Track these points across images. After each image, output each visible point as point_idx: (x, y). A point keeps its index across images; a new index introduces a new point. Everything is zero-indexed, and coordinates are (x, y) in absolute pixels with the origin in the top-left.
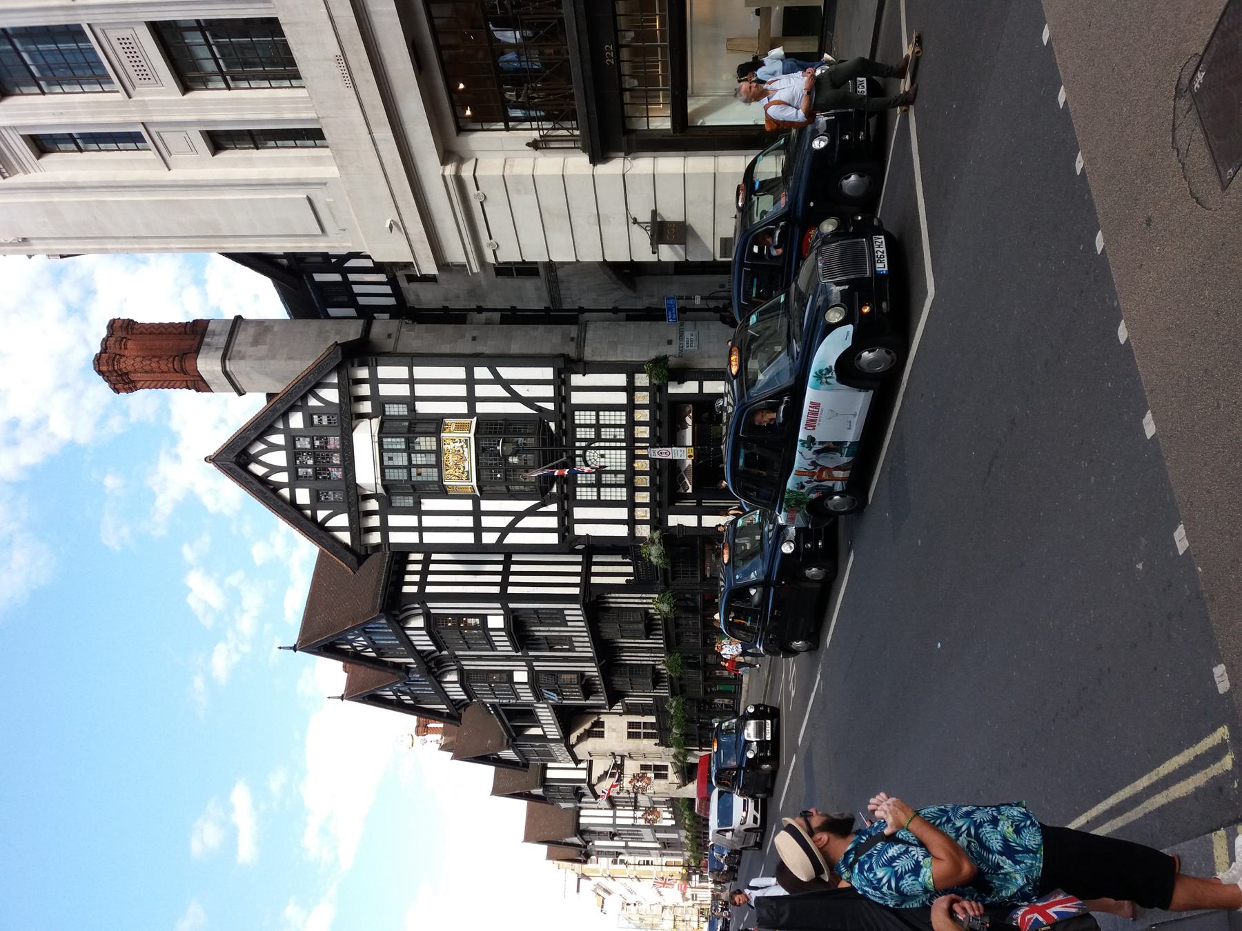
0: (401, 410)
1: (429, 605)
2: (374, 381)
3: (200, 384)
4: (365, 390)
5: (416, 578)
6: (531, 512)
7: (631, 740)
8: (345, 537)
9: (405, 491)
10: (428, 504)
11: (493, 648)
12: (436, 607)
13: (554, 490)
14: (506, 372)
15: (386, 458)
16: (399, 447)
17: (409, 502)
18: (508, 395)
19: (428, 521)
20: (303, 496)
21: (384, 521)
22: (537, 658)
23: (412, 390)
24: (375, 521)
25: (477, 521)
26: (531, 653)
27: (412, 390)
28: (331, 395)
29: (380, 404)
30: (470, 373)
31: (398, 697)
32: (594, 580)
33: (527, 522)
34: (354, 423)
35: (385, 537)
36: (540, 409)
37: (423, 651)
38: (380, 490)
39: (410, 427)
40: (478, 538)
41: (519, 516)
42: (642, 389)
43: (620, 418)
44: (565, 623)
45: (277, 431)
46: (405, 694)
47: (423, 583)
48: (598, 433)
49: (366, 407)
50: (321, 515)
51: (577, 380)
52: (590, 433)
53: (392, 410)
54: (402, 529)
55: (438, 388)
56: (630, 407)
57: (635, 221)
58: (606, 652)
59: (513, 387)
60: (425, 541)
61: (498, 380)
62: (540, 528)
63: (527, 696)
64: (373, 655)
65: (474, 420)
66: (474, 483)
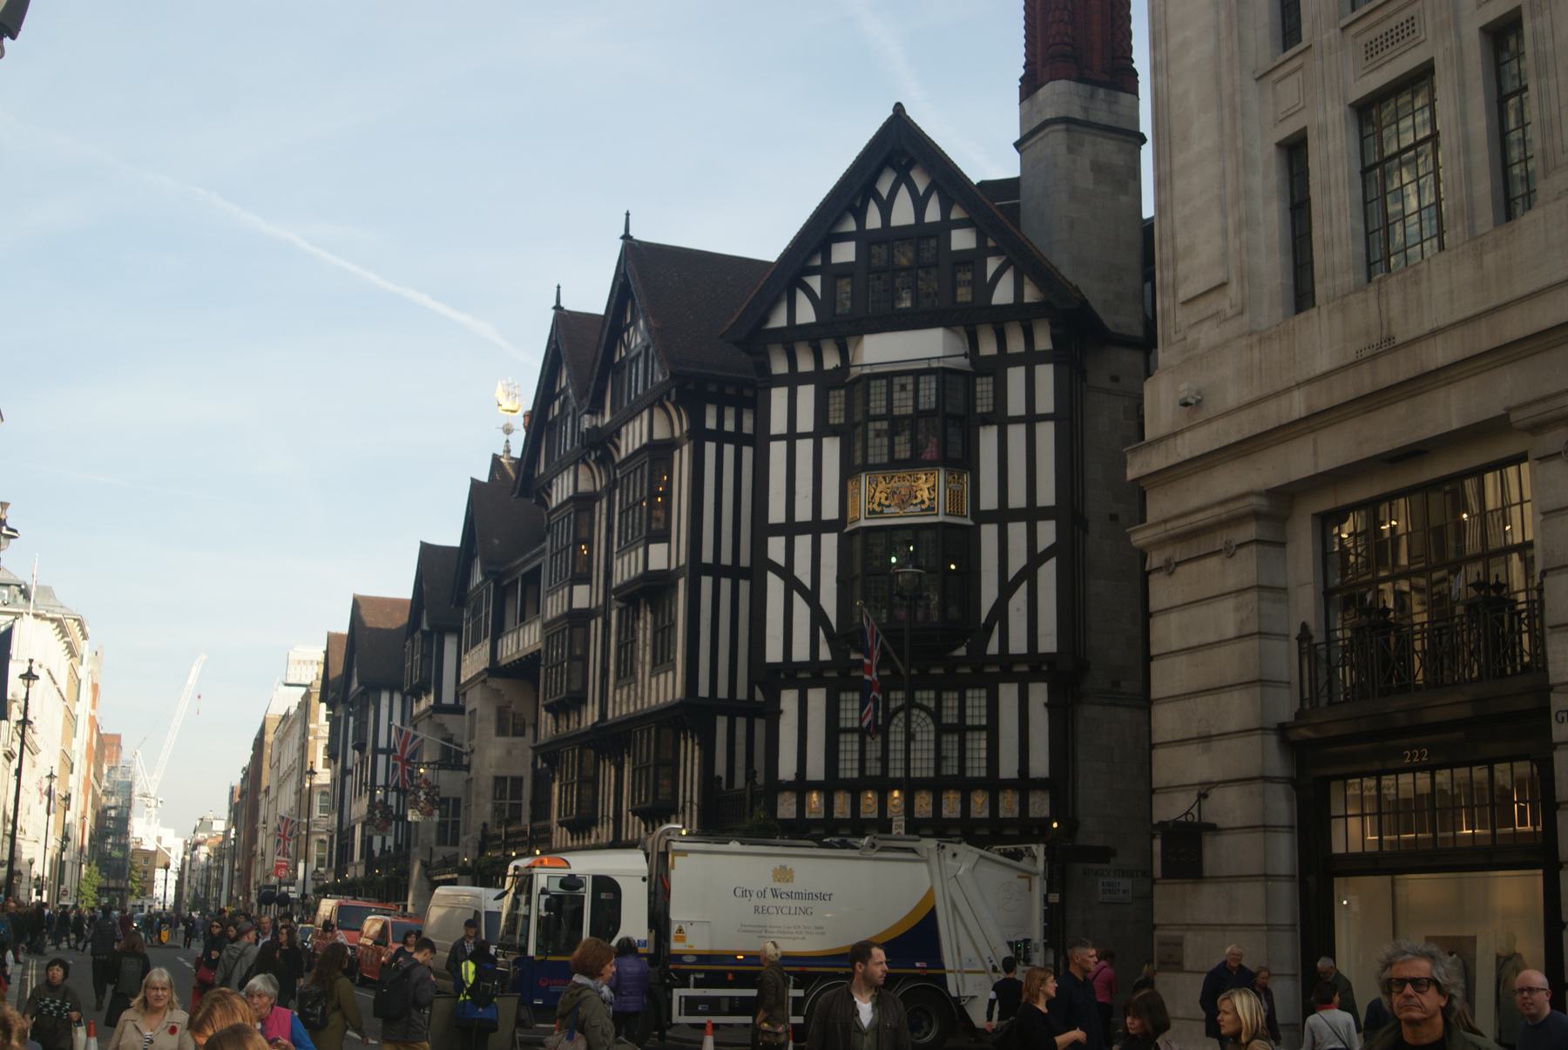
0: (984, 405)
1: (686, 448)
2: (1030, 359)
3: (1029, 86)
4: (1016, 345)
5: (729, 426)
6: (818, 617)
7: (491, 782)
8: (779, 320)
9: (853, 411)
10: (831, 447)
11: (621, 553)
12: (682, 460)
14: (1048, 574)
15: (903, 380)
16: (921, 400)
17: (836, 418)
18: (1012, 573)
19: (804, 448)
20: (844, 253)
21: (806, 379)
22: (607, 624)
23: (1017, 420)
24: (806, 364)
25: (803, 528)
26: (614, 614)
27: (1017, 420)
28: (1003, 294)
29: (995, 369)
30: (1046, 514)
31: (558, 396)
32: (722, 723)
33: (801, 609)
34: (961, 329)
35: (780, 381)
36: (988, 629)
37: (619, 437)
38: (855, 372)
39: (946, 424)
40: (777, 530)
41: (812, 597)
42: (1024, 805)
43: (977, 767)
44: (655, 672)
45: (945, 211)
46: (562, 407)
47: (720, 437)
48: (950, 729)
49: (988, 348)
50: (815, 282)
51: (1039, 693)
52: (950, 716)
53: (984, 387)
54: (792, 408)
55: (1019, 462)
56: (993, 784)
57: (1203, 796)
58: (612, 739)
59: (1024, 587)
60: (773, 444)
61: (1035, 559)
62: (789, 633)
63: (553, 606)
64: (617, 359)
65: (968, 522)
66: (864, 523)
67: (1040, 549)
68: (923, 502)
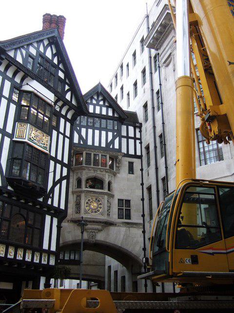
10: (13, 107)
13: (9, 188)
29: (58, 115)
59: (59, 185)
61: (62, 178)
66: (26, 140)
67: (63, 176)
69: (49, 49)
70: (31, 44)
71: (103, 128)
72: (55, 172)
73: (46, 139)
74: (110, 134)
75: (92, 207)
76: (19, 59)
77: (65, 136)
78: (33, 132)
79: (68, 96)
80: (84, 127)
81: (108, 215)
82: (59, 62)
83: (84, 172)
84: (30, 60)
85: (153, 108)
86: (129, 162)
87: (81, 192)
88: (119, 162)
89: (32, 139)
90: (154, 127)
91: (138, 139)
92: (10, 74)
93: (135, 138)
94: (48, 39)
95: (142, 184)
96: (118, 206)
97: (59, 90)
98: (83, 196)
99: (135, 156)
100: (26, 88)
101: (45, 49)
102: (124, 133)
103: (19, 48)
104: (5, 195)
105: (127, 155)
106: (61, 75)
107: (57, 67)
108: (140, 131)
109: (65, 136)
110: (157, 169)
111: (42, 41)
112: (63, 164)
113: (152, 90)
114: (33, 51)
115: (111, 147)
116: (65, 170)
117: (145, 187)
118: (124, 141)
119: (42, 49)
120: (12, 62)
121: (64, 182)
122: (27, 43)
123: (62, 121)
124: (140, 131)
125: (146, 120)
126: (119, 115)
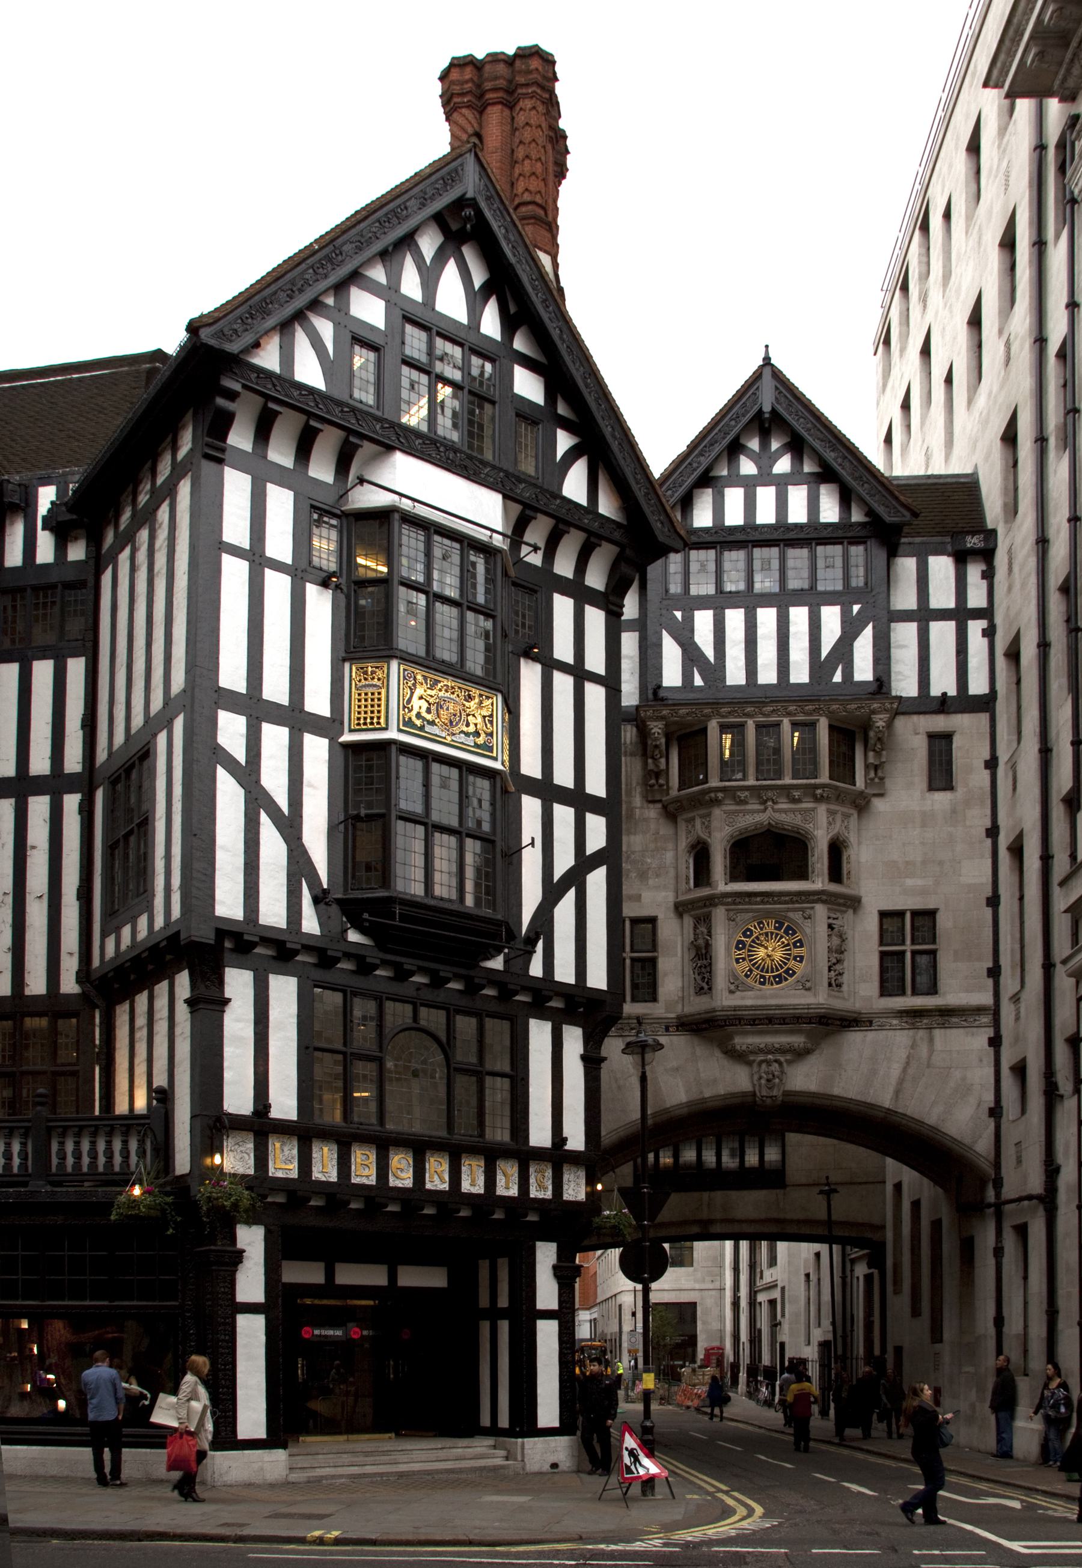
10: (320, 605)
59: (571, 895)
61: (584, 863)
66: (392, 734)
68: (477, 734)
69: (451, 272)
70: (355, 277)
71: (762, 595)
72: (548, 840)
73: (482, 709)
74: (831, 618)
75: (756, 964)
76: (309, 371)
77: (580, 674)
78: (419, 691)
79: (575, 486)
80: (703, 603)
81: (835, 985)
82: (509, 325)
83: (717, 812)
84: (361, 359)
85: (1041, 440)
86: (932, 736)
87: (712, 901)
88: (881, 744)
89: (418, 723)
90: (1043, 542)
91: (977, 614)
92: (281, 454)
93: (961, 615)
94: (439, 219)
95: (993, 832)
96: (881, 944)
97: (528, 467)
98: (719, 914)
99: (963, 702)
100: (368, 498)
101: (430, 280)
102: (905, 598)
103: (300, 316)
104: (345, 965)
105: (929, 704)
106: (527, 386)
107: (499, 355)
108: (989, 575)
109: (580, 674)
110: (1046, 752)
111: (408, 241)
112: (578, 799)
113: (1041, 341)
114: (368, 309)
115: (838, 678)
116: (597, 829)
117: (1004, 841)
118: (905, 634)
119: (411, 286)
120: (278, 398)
121: (597, 880)
122: (333, 279)
123: (563, 607)
124: (989, 575)
125: (1012, 509)
126: (870, 513)
